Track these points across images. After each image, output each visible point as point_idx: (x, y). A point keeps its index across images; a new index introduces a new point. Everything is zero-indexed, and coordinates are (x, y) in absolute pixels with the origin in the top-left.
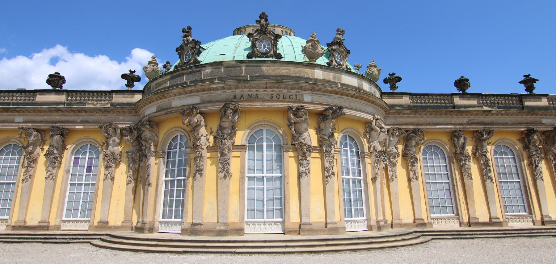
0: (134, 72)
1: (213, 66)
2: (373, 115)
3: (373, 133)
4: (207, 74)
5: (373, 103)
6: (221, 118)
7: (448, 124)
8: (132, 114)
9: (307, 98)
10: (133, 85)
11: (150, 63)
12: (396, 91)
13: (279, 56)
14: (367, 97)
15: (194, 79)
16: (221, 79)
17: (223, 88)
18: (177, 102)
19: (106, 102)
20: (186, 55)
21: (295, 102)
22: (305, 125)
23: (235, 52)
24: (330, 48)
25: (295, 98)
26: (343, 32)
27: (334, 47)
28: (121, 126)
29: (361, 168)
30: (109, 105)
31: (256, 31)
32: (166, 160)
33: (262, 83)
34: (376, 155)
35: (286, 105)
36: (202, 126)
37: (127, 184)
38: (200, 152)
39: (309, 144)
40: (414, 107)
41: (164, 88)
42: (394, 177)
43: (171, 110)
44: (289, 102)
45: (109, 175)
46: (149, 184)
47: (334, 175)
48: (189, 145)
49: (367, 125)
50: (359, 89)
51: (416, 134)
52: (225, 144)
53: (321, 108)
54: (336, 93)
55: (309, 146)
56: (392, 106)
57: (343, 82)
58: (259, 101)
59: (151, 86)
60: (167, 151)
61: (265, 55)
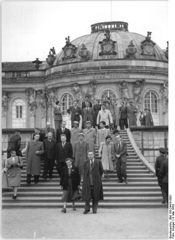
0: (38, 59)
6: (89, 88)
11: (49, 56)
22: (126, 90)
23: (93, 51)
27: (145, 44)
28: (36, 89)
29: (158, 108)
31: (104, 40)
35: (117, 80)
41: (60, 72)
44: (119, 79)
45: (32, 115)
53: (134, 81)
60: (62, 102)
61: (108, 53)
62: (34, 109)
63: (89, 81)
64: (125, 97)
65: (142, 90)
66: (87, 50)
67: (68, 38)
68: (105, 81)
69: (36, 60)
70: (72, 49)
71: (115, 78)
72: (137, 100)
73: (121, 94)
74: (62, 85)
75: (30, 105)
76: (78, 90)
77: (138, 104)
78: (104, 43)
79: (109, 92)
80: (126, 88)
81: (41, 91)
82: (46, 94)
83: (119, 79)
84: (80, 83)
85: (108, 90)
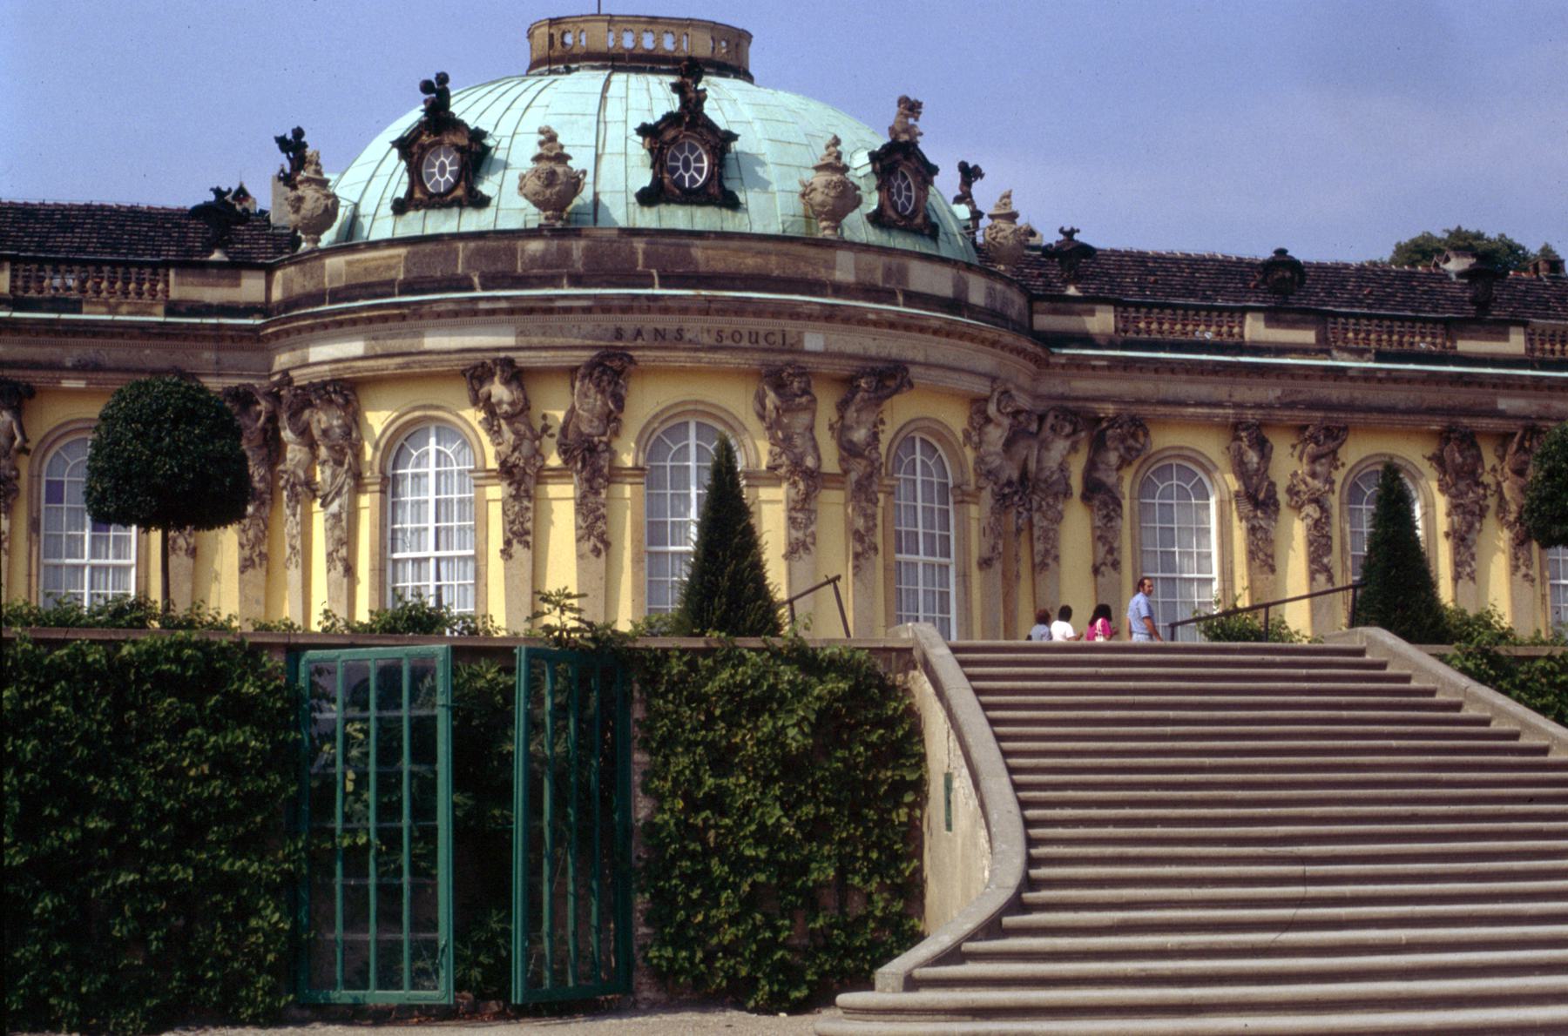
3: (990, 429)
4: (533, 260)
5: (994, 344)
7: (1219, 405)
16: (576, 281)
21: (781, 351)
22: (802, 419)
25: (779, 339)
37: (243, 569)
41: (391, 283)
42: (1049, 561)
43: (421, 358)
44: (765, 350)
46: (350, 570)
47: (876, 549)
48: (480, 464)
50: (956, 304)
58: (684, 349)
59: (323, 267)
63: (586, 355)
65: (881, 427)
66: (570, 163)
69: (211, 197)
70: (459, 149)
71: (745, 343)
74: (407, 365)
76: (512, 404)
78: (670, 134)
79: (699, 425)
82: (273, 419)
84: (523, 359)
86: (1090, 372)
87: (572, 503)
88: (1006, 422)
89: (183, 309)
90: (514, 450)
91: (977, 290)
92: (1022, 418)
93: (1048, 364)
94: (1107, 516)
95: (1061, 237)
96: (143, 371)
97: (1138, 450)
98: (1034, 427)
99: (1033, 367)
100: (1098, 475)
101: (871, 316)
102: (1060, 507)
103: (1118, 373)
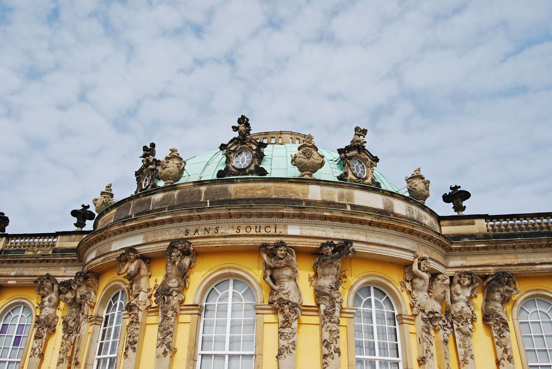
1: (165, 191)
2: (414, 252)
3: (416, 281)
4: (157, 203)
5: (411, 232)
8: (75, 263)
9: (293, 230)
10: (84, 225)
11: (102, 193)
12: (465, 213)
13: (263, 172)
14: (397, 224)
15: (139, 210)
17: (171, 221)
18: (118, 245)
19: (48, 248)
20: (146, 180)
21: (273, 236)
22: (288, 272)
24: (343, 155)
26: (365, 132)
28: (59, 280)
30: (51, 253)
31: (231, 141)
32: (102, 328)
33: (223, 211)
34: (423, 319)
35: (259, 241)
36: (143, 276)
38: (135, 314)
39: (295, 300)
40: (495, 236)
44: (264, 236)
49: (406, 270)
50: (385, 213)
51: (500, 283)
52: (168, 303)
53: (316, 244)
54: (341, 220)
55: (294, 306)
56: (458, 237)
57: (356, 203)
62: (45, 335)
64: (284, 297)
65: (344, 280)
67: (149, 147)
68: (218, 242)
72: (325, 311)
73: (272, 289)
74: (104, 260)
75: (38, 321)
77: (329, 324)
79: (234, 280)
80: (288, 266)
81: (67, 286)
83: (264, 236)
84: (143, 250)
85: (230, 275)
86: (476, 251)
87: (158, 325)
88: (427, 276)
89: (58, 251)
90: (135, 298)
91: (400, 208)
92: (440, 277)
93: (451, 250)
94: (500, 329)
95: (451, 191)
96: (36, 276)
97: (511, 292)
98: (448, 281)
99: (444, 252)
100: (490, 307)
101: (325, 214)
102: (471, 326)
103: (493, 251)
